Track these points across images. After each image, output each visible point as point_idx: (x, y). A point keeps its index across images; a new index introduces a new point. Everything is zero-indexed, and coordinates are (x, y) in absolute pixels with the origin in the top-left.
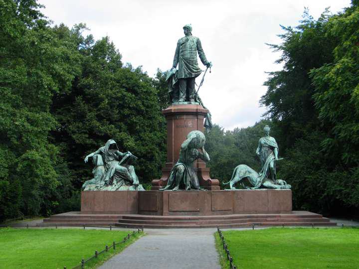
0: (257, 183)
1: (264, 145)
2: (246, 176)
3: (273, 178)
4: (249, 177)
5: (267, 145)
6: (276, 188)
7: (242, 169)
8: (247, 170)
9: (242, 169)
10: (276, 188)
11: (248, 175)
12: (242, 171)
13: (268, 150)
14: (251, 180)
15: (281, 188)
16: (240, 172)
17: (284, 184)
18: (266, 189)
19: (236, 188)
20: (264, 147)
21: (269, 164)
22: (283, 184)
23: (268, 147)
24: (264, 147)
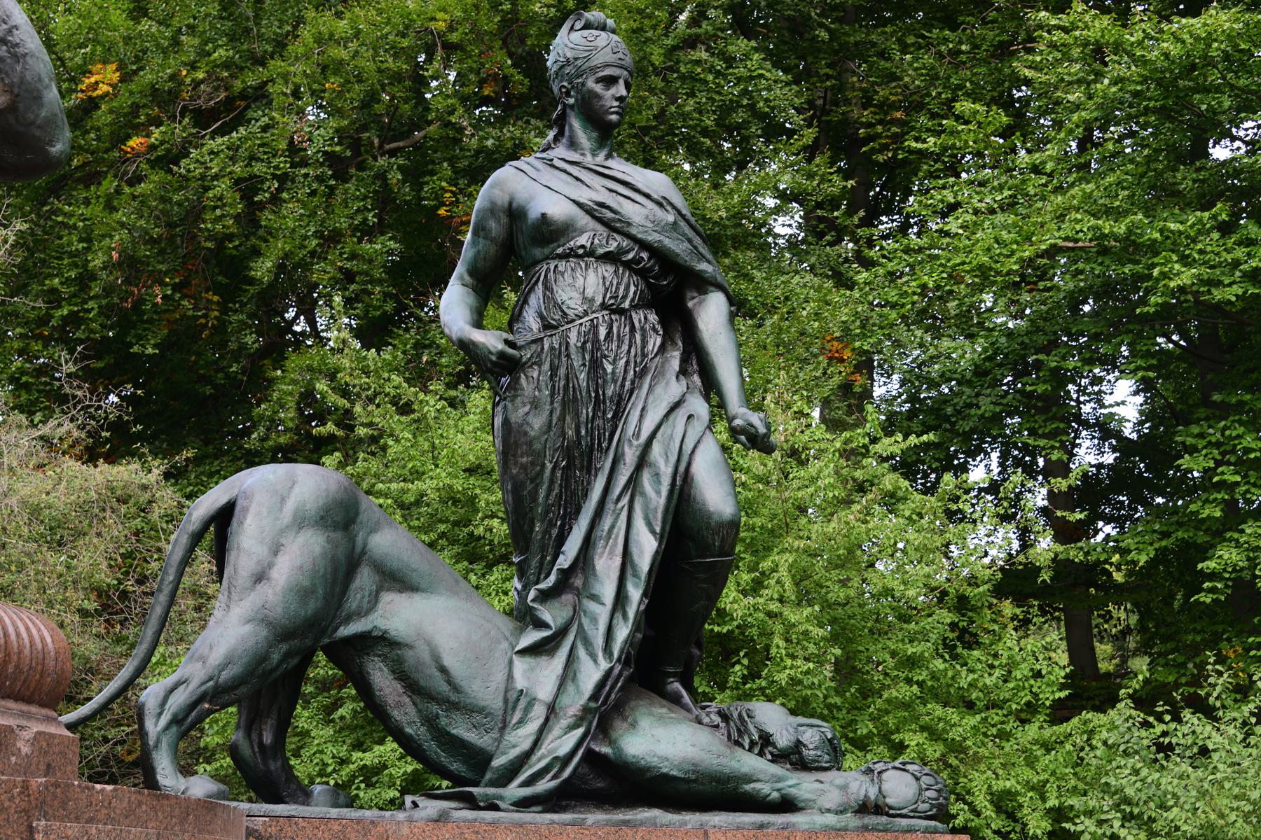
0: (521, 738)
6: (787, 805)
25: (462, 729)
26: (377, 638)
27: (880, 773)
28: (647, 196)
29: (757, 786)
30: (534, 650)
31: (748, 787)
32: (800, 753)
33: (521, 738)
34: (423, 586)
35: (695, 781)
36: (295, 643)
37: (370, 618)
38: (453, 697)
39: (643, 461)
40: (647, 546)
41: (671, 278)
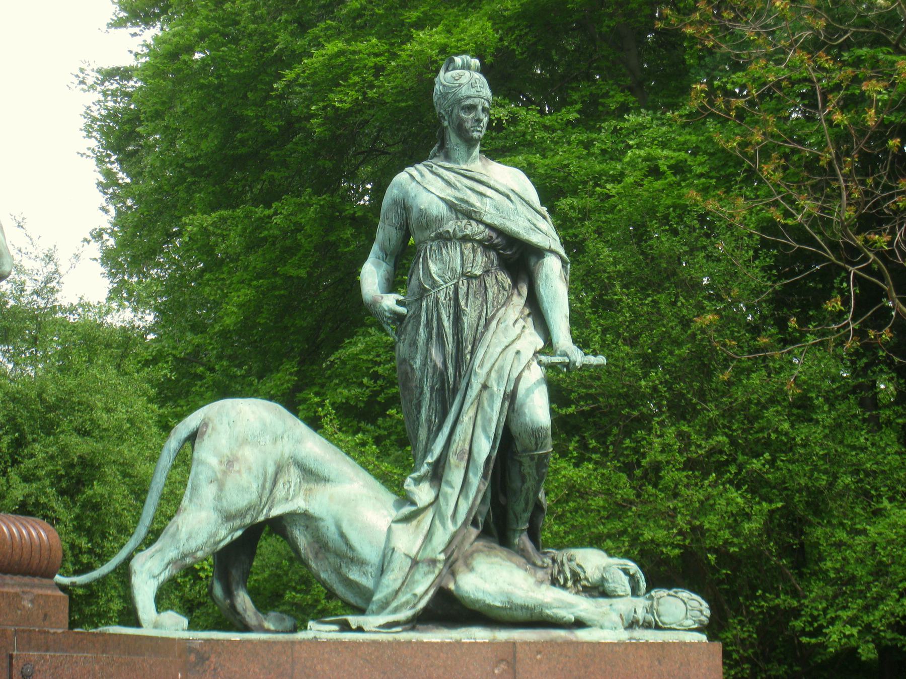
1: (450, 226)
2: (276, 512)
3: (523, 540)
4: (307, 519)
5: (473, 229)
6: (579, 624)
7: (245, 442)
8: (286, 448)
9: (245, 442)
10: (579, 624)
11: (299, 504)
12: (249, 454)
13: (487, 272)
14: (321, 545)
15: (632, 624)
16: (230, 463)
17: (635, 592)
18: (502, 635)
19: (192, 626)
20: (445, 238)
21: (511, 397)
22: (622, 584)
23: (487, 246)
24: (445, 238)
25: (354, 575)
26: (300, 514)
27: (658, 599)
28: (497, 191)
29: (555, 611)
30: (407, 519)
31: (548, 612)
32: (603, 586)
33: (392, 580)
34: (332, 477)
35: (511, 609)
36: (237, 522)
37: (295, 501)
38: (350, 554)
39: (485, 387)
40: (484, 448)
41: (514, 250)
